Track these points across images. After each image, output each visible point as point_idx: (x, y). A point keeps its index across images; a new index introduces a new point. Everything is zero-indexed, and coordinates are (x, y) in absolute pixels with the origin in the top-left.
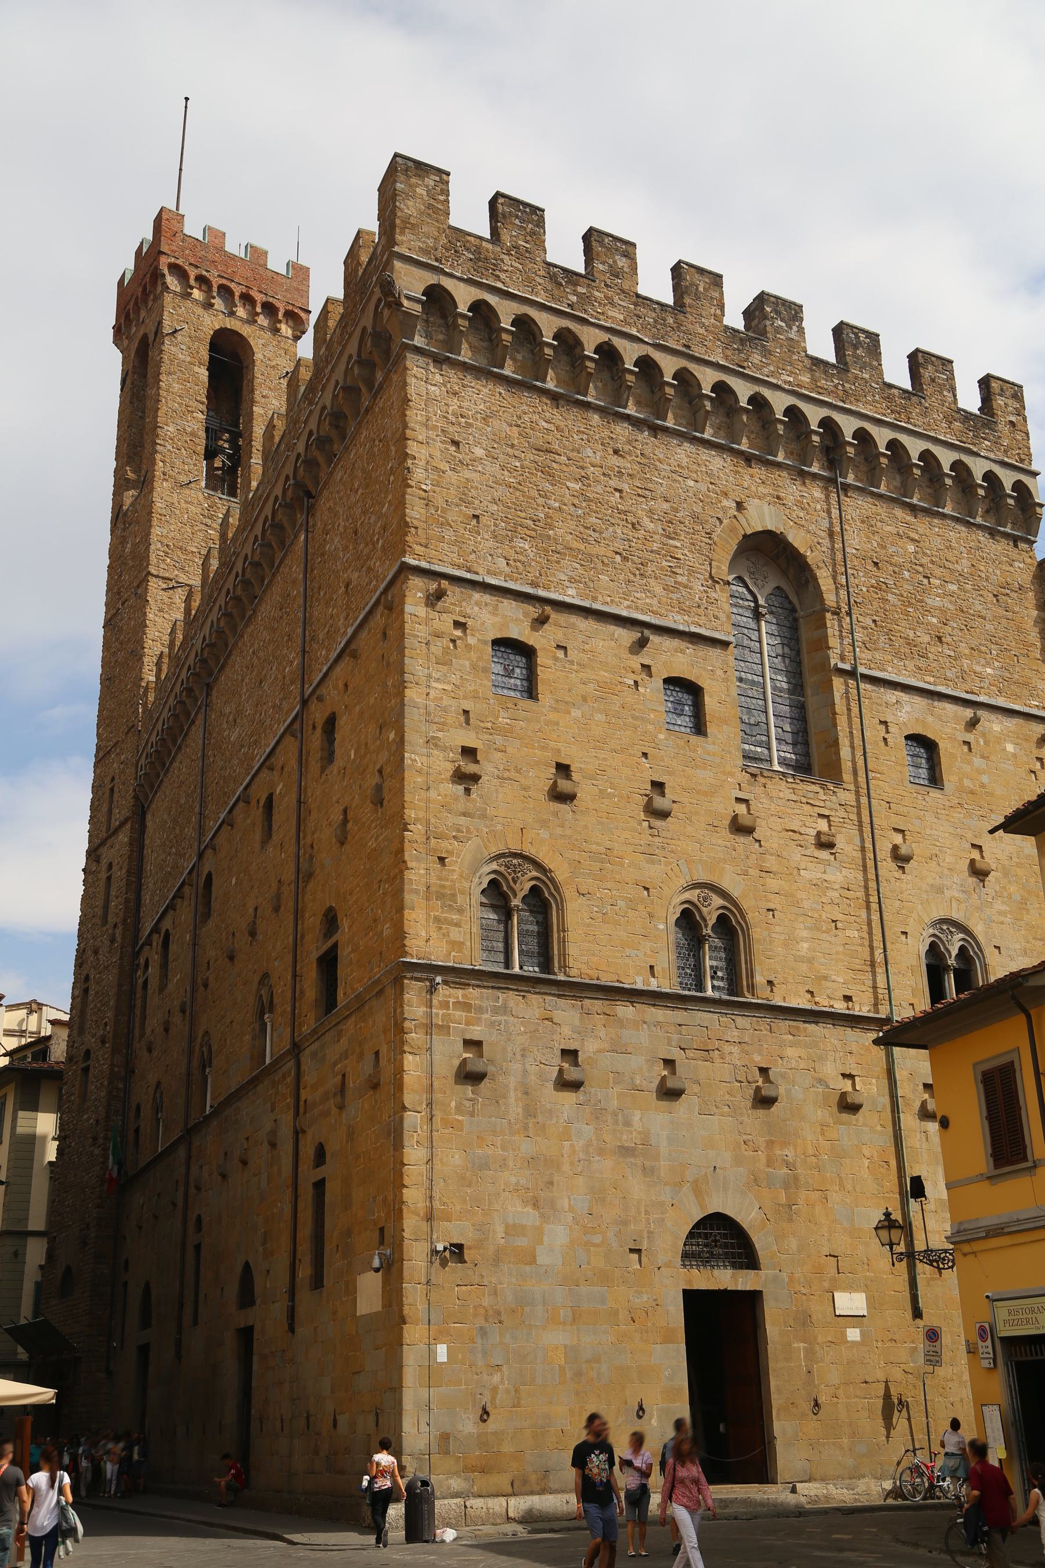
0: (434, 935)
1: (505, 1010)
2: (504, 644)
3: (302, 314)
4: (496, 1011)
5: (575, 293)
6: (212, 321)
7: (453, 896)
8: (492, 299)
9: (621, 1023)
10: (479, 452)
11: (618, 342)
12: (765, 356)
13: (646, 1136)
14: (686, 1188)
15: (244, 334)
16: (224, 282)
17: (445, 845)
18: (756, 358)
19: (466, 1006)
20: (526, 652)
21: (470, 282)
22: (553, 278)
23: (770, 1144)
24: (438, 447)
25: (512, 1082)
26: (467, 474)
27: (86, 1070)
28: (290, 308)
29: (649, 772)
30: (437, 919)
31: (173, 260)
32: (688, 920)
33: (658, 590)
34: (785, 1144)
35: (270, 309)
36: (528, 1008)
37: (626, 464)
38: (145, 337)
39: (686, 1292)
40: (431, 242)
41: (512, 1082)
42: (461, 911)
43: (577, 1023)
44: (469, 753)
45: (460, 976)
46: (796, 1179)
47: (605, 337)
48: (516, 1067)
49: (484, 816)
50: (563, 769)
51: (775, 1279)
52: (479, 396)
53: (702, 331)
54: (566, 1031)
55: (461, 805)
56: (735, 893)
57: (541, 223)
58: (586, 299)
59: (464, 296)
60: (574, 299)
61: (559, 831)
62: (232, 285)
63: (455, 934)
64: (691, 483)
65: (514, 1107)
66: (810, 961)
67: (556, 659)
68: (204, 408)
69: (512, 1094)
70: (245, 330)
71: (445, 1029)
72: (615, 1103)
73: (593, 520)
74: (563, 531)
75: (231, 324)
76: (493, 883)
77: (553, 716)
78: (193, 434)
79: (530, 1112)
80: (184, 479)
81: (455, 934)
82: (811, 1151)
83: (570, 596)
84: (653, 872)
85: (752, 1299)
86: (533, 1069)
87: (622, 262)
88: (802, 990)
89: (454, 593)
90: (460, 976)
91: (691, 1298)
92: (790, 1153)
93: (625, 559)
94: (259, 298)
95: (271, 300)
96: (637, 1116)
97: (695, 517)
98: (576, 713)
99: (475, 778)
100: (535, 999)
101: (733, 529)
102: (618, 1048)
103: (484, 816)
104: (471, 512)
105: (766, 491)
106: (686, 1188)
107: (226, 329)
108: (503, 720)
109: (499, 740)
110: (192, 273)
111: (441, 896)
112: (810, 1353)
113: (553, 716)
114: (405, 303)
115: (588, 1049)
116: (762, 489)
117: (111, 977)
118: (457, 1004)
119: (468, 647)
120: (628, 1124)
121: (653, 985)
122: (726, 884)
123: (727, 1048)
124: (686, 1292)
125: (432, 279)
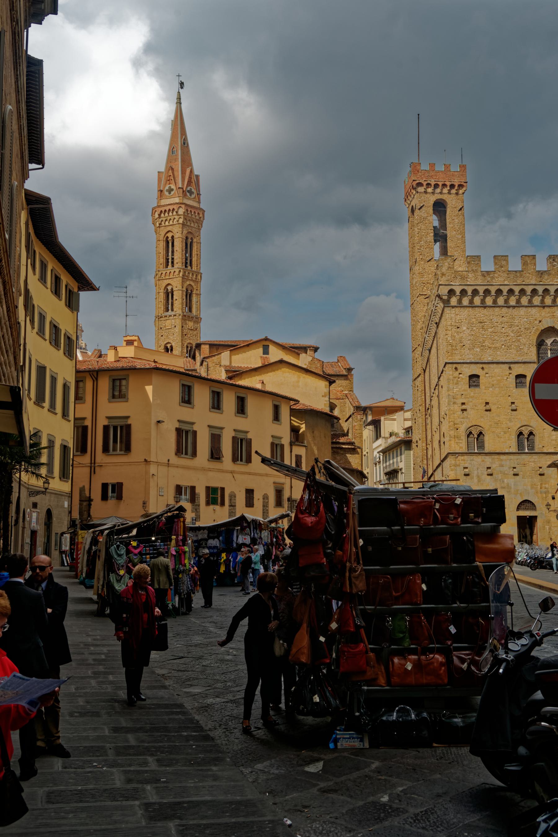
0: (456, 446)
1: (473, 460)
2: (471, 377)
3: (465, 184)
4: (471, 460)
5: (490, 277)
6: (432, 199)
7: (460, 437)
8: (466, 288)
9: (502, 460)
10: (465, 328)
11: (501, 288)
12: (549, 276)
13: (508, 484)
14: (518, 495)
15: (444, 198)
16: (436, 182)
17: (458, 426)
18: (546, 277)
19: (464, 460)
20: (478, 376)
21: (460, 285)
22: (483, 275)
23: (541, 484)
24: (454, 330)
25: (475, 475)
26: (461, 335)
27: (417, 446)
28: (460, 183)
29: (511, 400)
30: (457, 443)
31: (418, 181)
32: (521, 434)
33: (515, 352)
34: (545, 484)
35: (452, 186)
36: (478, 459)
37: (505, 319)
38: (412, 206)
39: (518, 516)
40: (449, 278)
41: (475, 475)
42: (462, 440)
43: (491, 461)
44: (463, 404)
45: (462, 454)
46: (548, 491)
47: (497, 287)
48: (476, 472)
49: (467, 418)
50: (487, 403)
51: (541, 513)
52: (465, 313)
53: (528, 275)
54: (488, 463)
55: (462, 416)
56: (534, 426)
57: (480, 261)
58: (493, 278)
59: (458, 290)
60: (489, 279)
61: (486, 418)
62: (438, 183)
63: (461, 445)
64: (525, 319)
65: (475, 480)
66: (556, 440)
67: (485, 377)
68: (432, 231)
69: (475, 478)
70: (445, 197)
71: (459, 465)
72: (500, 478)
73: (496, 338)
74: (486, 343)
75: (439, 197)
76: (471, 433)
77: (485, 391)
78: (430, 242)
79: (479, 481)
80: (428, 259)
81: (461, 445)
82: (553, 485)
83: (490, 359)
84: (510, 424)
85: (536, 517)
86: (480, 472)
87: (504, 263)
88: (553, 448)
89: (458, 366)
90: (462, 454)
91: (519, 518)
92: (547, 486)
93: (505, 346)
94: (448, 184)
95: (453, 183)
96: (506, 480)
97: (525, 329)
98: (491, 389)
99: (465, 410)
100: (480, 457)
101: (537, 329)
102: (502, 466)
103: (467, 418)
104: (462, 345)
105: (549, 315)
106: (518, 495)
107: (437, 200)
108: (472, 394)
109: (470, 399)
110: (425, 183)
111: (457, 437)
112: (550, 529)
113: (485, 391)
114: (444, 297)
115: (493, 466)
116: (549, 315)
117: (420, 420)
118: (462, 460)
119: (463, 379)
120: (503, 482)
121: (511, 451)
122: (531, 425)
123: (530, 463)
124: (518, 516)
125: (449, 288)
